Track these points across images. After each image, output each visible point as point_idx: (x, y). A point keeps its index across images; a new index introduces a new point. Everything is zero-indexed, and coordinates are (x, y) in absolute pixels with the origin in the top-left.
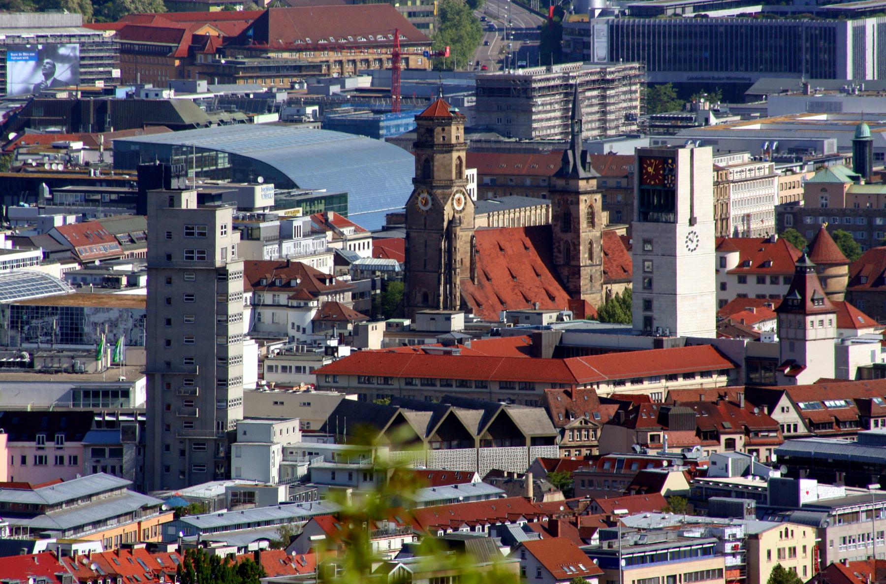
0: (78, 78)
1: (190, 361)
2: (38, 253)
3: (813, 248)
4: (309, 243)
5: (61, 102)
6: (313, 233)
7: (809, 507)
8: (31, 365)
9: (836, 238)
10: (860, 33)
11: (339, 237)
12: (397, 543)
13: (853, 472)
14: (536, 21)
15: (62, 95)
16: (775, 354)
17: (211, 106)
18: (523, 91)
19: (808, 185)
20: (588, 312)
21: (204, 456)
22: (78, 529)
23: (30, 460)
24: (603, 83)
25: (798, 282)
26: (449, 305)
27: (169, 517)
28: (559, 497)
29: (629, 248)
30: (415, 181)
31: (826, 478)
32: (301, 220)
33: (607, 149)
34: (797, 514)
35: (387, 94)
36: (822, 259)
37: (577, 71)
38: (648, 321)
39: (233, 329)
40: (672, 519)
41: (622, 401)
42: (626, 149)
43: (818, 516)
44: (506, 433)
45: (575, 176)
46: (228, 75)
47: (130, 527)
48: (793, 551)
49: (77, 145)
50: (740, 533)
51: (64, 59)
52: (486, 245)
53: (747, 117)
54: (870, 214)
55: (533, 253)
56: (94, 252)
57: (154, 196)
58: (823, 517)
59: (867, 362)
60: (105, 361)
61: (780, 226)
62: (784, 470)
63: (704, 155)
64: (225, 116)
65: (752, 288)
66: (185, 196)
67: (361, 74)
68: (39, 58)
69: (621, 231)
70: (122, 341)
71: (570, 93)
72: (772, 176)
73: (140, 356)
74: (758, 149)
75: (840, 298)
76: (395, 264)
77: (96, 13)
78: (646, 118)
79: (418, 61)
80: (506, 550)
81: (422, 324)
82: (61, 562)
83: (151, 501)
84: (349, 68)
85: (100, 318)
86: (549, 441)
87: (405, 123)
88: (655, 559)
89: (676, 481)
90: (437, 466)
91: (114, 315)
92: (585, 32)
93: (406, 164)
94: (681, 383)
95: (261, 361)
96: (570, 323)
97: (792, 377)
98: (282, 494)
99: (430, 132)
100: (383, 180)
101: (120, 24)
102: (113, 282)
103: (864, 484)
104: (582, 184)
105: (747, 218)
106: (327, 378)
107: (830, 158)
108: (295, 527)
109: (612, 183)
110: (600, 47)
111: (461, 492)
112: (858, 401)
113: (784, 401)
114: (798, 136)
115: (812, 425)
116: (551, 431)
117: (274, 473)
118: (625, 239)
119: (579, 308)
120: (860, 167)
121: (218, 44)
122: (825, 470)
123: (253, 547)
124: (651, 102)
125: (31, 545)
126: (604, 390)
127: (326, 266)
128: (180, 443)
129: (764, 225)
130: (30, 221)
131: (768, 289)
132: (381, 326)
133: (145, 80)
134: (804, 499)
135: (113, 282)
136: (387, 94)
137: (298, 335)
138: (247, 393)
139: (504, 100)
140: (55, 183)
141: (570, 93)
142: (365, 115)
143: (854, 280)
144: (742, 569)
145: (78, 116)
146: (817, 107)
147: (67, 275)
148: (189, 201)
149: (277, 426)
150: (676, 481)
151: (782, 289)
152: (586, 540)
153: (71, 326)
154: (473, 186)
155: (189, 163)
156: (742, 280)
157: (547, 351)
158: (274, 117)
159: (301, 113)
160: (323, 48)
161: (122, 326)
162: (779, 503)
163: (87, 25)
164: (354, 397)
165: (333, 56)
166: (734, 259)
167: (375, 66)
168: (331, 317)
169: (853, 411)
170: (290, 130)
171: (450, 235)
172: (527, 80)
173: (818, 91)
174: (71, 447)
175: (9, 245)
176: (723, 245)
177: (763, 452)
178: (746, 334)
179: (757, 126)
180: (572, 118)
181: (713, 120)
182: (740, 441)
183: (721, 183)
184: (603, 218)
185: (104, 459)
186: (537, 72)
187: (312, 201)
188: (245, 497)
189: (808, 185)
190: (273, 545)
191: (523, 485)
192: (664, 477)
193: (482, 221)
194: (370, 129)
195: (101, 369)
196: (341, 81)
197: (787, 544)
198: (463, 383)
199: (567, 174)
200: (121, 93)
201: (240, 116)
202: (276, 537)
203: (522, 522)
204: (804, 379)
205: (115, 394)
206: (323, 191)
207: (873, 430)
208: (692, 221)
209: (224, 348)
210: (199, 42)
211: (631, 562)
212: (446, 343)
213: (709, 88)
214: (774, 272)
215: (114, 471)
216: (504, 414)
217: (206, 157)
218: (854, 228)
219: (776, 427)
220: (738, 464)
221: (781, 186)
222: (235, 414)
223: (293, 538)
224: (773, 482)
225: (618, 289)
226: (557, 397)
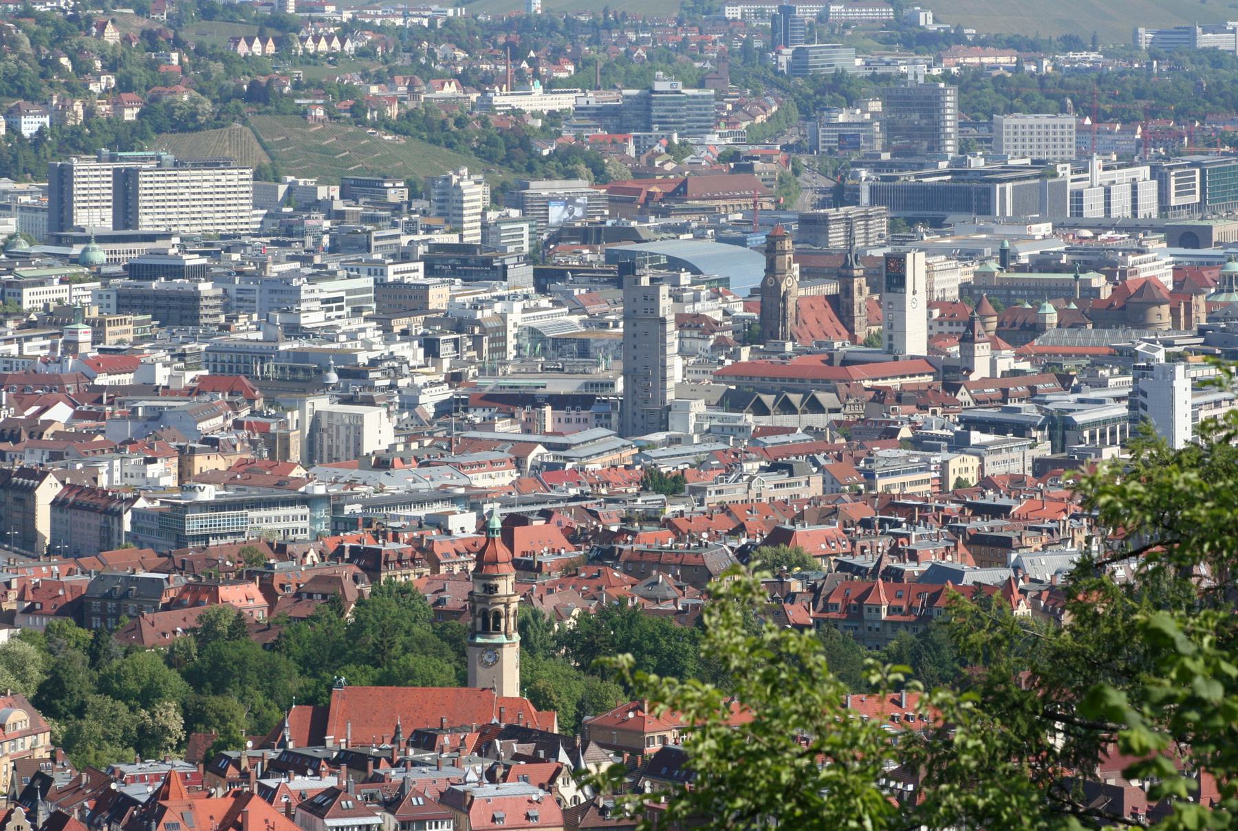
0: (586, 215)
1: (646, 367)
2: (566, 310)
3: (978, 306)
4: (710, 304)
5: (578, 228)
6: (711, 299)
7: (975, 446)
8: (562, 370)
9: (990, 302)
10: (1003, 191)
11: (725, 301)
12: (757, 465)
13: (998, 427)
14: (831, 184)
15: (578, 225)
16: (958, 364)
17: (656, 230)
18: (824, 221)
19: (975, 273)
20: (858, 341)
21: (655, 419)
22: (588, 457)
23: (563, 420)
24: (867, 217)
25: (970, 325)
26: (784, 338)
27: (636, 451)
28: (843, 441)
29: (881, 307)
30: (766, 271)
31: (984, 430)
32: (705, 292)
33: (868, 253)
34: (969, 450)
35: (751, 223)
36: (984, 313)
37: (852, 211)
38: (891, 346)
39: (669, 351)
40: (903, 452)
41: (877, 390)
42: (879, 253)
43: (980, 451)
44: (815, 406)
45: (852, 268)
46: (666, 213)
47: (616, 456)
48: (967, 469)
49: (586, 251)
50: (939, 460)
51: (579, 205)
52: (804, 305)
53: (943, 236)
54: (1009, 289)
55: (829, 309)
56: (595, 309)
57: (627, 279)
58: (982, 451)
59: (1007, 369)
60: (602, 367)
61: (961, 295)
62: (962, 426)
63: (921, 256)
64: (664, 235)
65: (946, 329)
66: (643, 279)
67: (736, 212)
68: (566, 204)
69: (876, 297)
70: (610, 357)
71: (849, 223)
72: (957, 268)
73: (619, 365)
74: (949, 254)
75: (993, 333)
76: (755, 315)
77: (596, 180)
78: (889, 236)
79: (767, 206)
80: (815, 470)
81: (770, 348)
82: (580, 474)
83: (626, 442)
84: (730, 209)
85: (599, 344)
86: (837, 411)
87: (760, 239)
88: (893, 474)
89: (905, 432)
90: (778, 424)
91: (606, 343)
92: (856, 190)
93: (761, 263)
94: (908, 380)
95: (684, 368)
96: (849, 347)
97: (967, 377)
98: (696, 439)
99: (774, 244)
100: (748, 270)
101: (608, 186)
102: (606, 325)
103: (1004, 434)
104: (855, 272)
105: (944, 290)
106: (719, 377)
107: (987, 258)
108: (703, 457)
109: (871, 271)
110: (865, 197)
111: (791, 438)
112: (1002, 389)
113: (963, 389)
114: (970, 247)
115: (977, 402)
116: (839, 405)
117: (691, 427)
118: (878, 302)
119: (853, 339)
120: (1003, 263)
121: (661, 196)
122: (984, 426)
123: (681, 467)
124: (892, 227)
125: (564, 466)
126: (867, 384)
127: (718, 316)
128: (642, 413)
129: (953, 294)
130: (561, 292)
131: (954, 329)
132: (748, 349)
133: (622, 216)
134: (973, 442)
135: (606, 325)
136: (751, 223)
137: (704, 354)
138: (677, 385)
139: (813, 226)
140: (574, 272)
141: (849, 223)
142: (738, 234)
143: (1000, 324)
144: (940, 479)
145: (587, 236)
146: (980, 231)
147: (581, 321)
148: (645, 282)
149: (693, 403)
150: (905, 432)
151: (962, 329)
152: (857, 464)
153: (584, 349)
154: (797, 273)
155: (645, 261)
156: (941, 324)
157: (837, 362)
158: (690, 236)
159: (704, 234)
160: (716, 199)
161: (610, 349)
162: (959, 444)
163: (591, 186)
164: (734, 387)
165: (722, 203)
166: (936, 313)
167: (744, 208)
168: (721, 345)
169: (999, 395)
170: (699, 243)
171: (784, 300)
172: (826, 216)
173: (981, 222)
174: (584, 414)
175: (551, 305)
176: (931, 305)
177: (951, 416)
178: (943, 354)
179: (949, 241)
180: (850, 236)
181: (925, 238)
182: (939, 410)
183: (930, 272)
184: (867, 290)
185: (602, 420)
186: (831, 211)
187: (710, 281)
188: (677, 441)
189: (975, 273)
190: (692, 466)
191: (824, 435)
192: (898, 430)
193: (802, 292)
194: (741, 242)
195: (599, 373)
196: (726, 216)
197: (963, 465)
198: (792, 380)
199: (847, 266)
200: (609, 223)
201: (672, 235)
202: (693, 462)
203: (823, 454)
204: (974, 377)
205: (607, 385)
206: (717, 276)
207: (1010, 405)
208: (914, 292)
209: (664, 361)
210: (651, 195)
211: (881, 475)
212: (782, 358)
213: (923, 220)
214: (958, 320)
215: (608, 426)
216: (813, 397)
217: (654, 258)
218: (1000, 296)
219: (959, 403)
220: (938, 423)
221: (963, 273)
222: (670, 396)
223: (702, 463)
224: (956, 433)
225: (874, 329)
226: (842, 387)
